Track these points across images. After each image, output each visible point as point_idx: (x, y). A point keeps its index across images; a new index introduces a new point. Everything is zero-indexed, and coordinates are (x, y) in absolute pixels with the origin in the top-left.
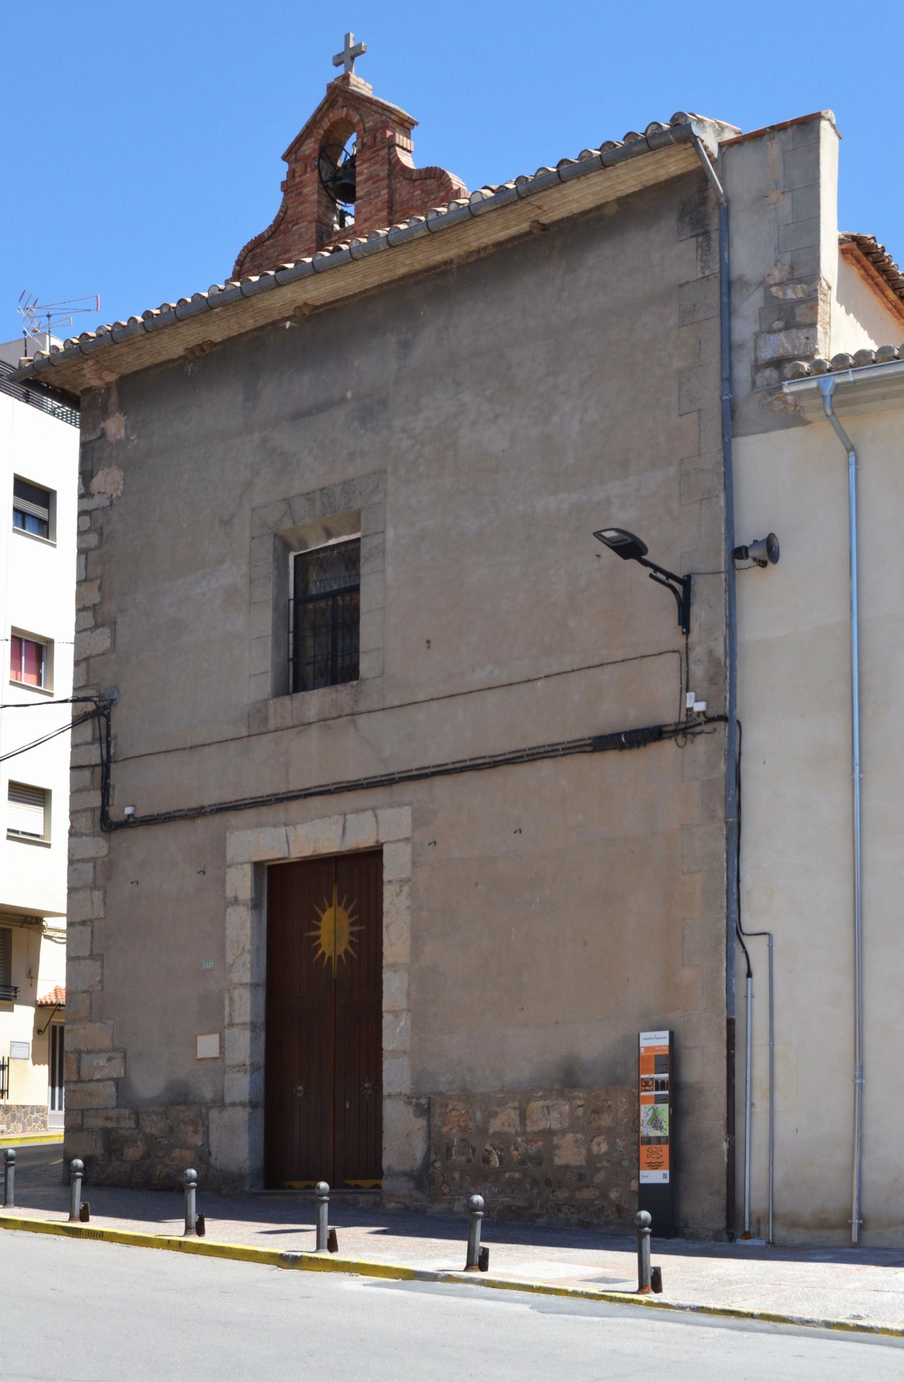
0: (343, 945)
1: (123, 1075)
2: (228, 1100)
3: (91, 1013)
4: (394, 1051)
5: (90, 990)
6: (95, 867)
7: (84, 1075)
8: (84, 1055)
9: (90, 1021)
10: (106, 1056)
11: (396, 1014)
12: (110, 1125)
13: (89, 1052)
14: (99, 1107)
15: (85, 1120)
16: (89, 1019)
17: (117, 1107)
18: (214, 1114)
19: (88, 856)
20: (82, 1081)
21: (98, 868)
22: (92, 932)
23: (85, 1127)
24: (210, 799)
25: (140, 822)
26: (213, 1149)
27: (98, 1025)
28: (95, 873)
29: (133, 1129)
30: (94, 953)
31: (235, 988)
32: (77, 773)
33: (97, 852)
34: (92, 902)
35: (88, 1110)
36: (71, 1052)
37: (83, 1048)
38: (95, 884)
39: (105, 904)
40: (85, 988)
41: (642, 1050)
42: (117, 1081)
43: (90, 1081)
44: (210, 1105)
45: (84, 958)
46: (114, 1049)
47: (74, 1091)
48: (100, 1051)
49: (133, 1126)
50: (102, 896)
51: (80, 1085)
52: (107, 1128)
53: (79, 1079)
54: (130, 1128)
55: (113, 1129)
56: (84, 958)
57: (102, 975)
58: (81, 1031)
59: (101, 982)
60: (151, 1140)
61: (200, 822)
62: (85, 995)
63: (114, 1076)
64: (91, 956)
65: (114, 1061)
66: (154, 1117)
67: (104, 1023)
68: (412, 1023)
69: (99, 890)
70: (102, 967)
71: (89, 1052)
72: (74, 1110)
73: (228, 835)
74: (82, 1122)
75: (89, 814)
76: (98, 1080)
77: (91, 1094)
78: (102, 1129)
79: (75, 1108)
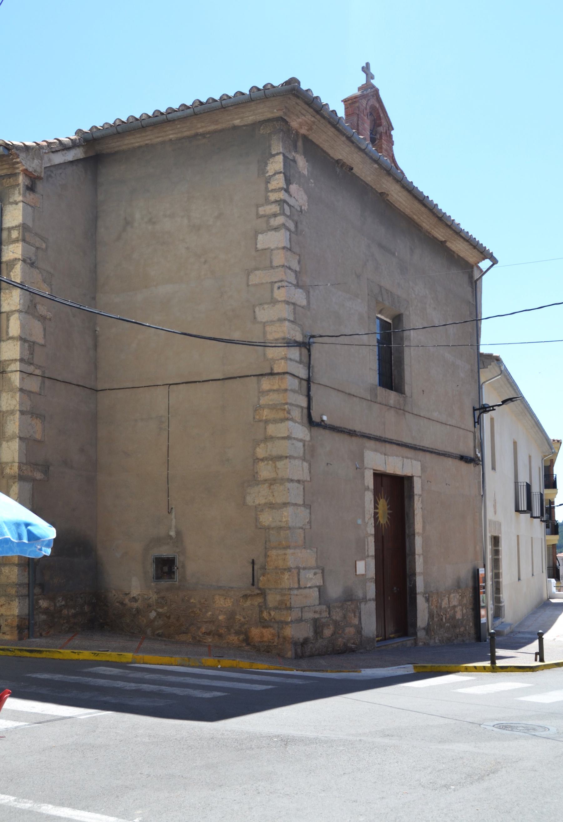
0: (386, 519)
1: (322, 584)
2: (368, 598)
3: (305, 542)
4: (419, 573)
5: (304, 527)
6: (304, 446)
7: (302, 584)
8: (301, 571)
9: (305, 548)
10: (313, 571)
11: (419, 555)
12: (317, 616)
13: (304, 569)
14: (311, 605)
15: (303, 615)
16: (304, 547)
17: (320, 604)
18: (363, 606)
19: (300, 438)
20: (301, 588)
21: (306, 447)
22: (304, 489)
23: (303, 619)
24: (358, 427)
25: (329, 427)
26: (363, 625)
27: (308, 551)
28: (304, 450)
29: (328, 618)
30: (305, 503)
31: (369, 536)
32: (291, 378)
33: (304, 437)
34: (303, 469)
35: (304, 607)
36: (294, 568)
37: (301, 566)
38: (305, 458)
39: (310, 472)
40: (301, 525)
41: (480, 575)
42: (319, 587)
43: (305, 588)
44: (361, 601)
45: (300, 505)
46: (318, 567)
47: (297, 595)
48: (310, 568)
49: (328, 616)
50: (308, 467)
51: (300, 591)
52: (315, 618)
53: (299, 587)
54: (326, 617)
55: (318, 618)
56: (300, 505)
57: (310, 518)
58: (299, 554)
59: (310, 522)
60: (336, 623)
61: (354, 439)
62: (301, 530)
63: (318, 584)
64: (304, 505)
65: (317, 575)
66: (337, 610)
67: (312, 550)
68: (424, 560)
69: (307, 462)
70: (310, 514)
71: (304, 569)
72: (297, 608)
73: (365, 451)
74: (302, 616)
75: (300, 410)
76: (310, 587)
77: (306, 597)
78: (313, 619)
79: (298, 606)
